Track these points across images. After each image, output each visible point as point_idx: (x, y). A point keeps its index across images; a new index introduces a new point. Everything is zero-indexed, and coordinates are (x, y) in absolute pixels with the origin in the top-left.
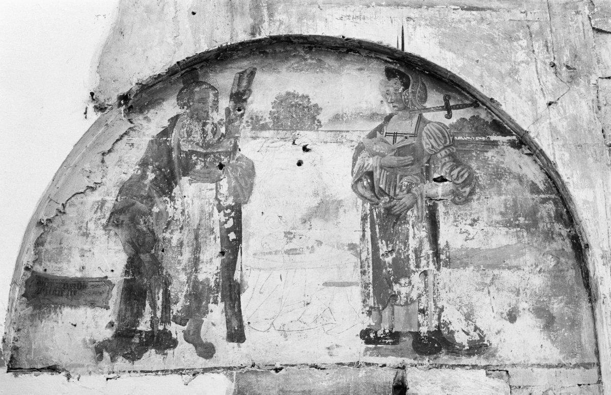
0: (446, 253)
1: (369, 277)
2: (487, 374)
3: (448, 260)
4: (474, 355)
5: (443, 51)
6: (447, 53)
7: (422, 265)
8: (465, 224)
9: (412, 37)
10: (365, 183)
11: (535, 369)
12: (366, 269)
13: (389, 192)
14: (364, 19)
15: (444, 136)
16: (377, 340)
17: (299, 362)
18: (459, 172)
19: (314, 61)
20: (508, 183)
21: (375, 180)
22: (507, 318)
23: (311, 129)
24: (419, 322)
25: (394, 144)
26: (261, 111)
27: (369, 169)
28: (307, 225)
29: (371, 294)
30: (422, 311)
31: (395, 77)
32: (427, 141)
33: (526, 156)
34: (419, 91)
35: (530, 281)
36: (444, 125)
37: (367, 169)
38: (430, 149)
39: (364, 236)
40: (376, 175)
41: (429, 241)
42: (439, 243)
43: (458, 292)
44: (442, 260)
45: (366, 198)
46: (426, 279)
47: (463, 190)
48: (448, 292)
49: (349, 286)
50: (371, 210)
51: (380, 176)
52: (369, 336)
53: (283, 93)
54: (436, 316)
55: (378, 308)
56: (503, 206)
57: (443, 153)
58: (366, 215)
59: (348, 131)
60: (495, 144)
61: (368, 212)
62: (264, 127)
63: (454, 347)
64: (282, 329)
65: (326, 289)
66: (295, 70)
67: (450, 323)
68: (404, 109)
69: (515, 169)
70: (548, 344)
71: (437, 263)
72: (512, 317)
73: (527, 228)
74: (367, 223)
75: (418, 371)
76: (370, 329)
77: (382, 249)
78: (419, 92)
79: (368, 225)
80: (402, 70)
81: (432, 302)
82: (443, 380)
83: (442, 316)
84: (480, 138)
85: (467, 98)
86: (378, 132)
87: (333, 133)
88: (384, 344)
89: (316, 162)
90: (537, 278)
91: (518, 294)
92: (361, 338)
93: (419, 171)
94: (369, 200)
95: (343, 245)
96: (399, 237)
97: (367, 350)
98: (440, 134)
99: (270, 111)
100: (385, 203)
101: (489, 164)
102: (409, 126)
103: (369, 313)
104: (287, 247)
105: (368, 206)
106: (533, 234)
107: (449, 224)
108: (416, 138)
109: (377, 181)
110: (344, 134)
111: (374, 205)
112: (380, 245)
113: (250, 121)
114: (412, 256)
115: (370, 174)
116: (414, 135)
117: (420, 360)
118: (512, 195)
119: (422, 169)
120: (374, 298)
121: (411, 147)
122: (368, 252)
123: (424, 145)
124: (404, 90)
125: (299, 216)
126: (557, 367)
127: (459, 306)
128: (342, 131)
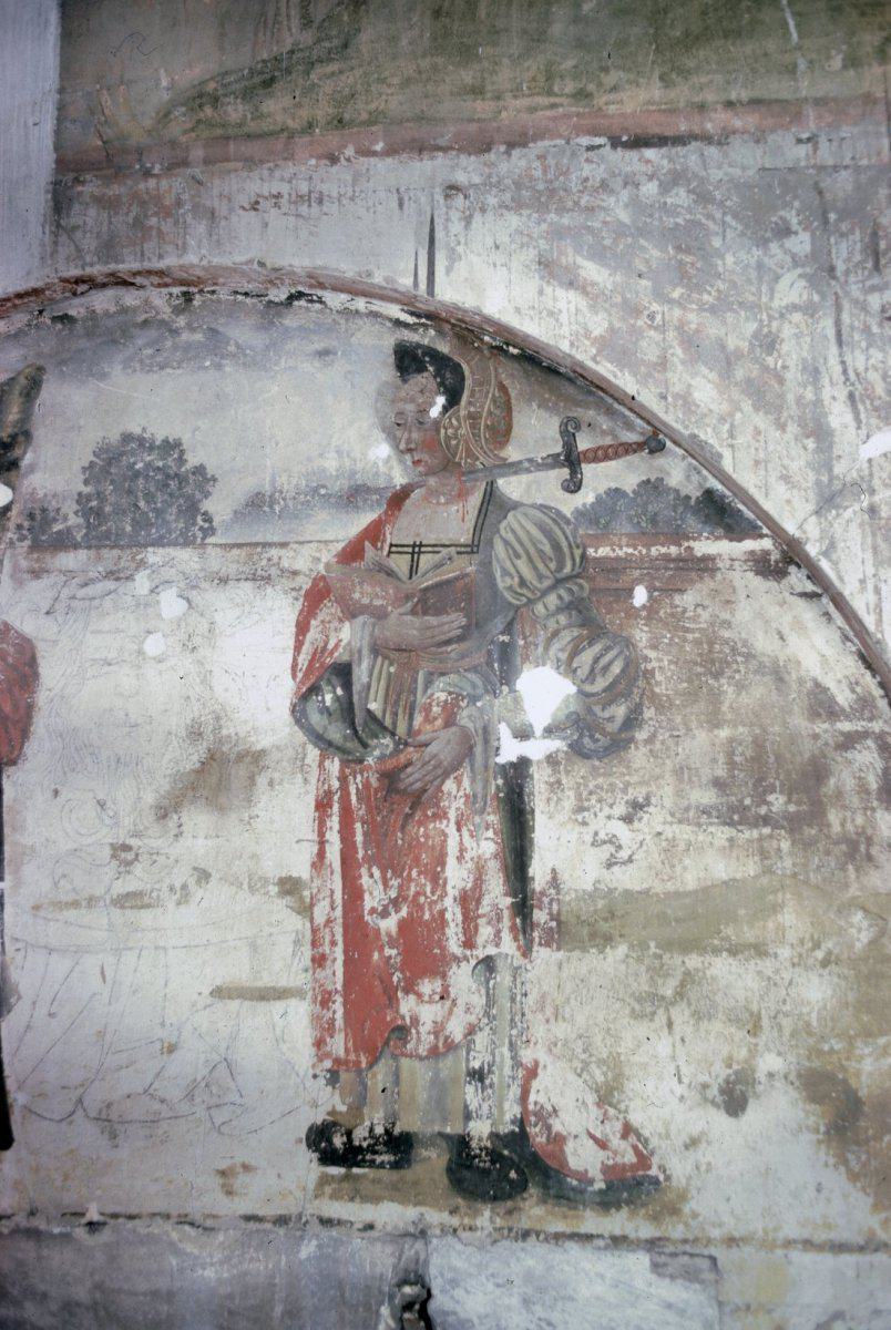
0: (550, 903)
1: (334, 974)
2: (655, 1267)
3: (554, 924)
4: (618, 1208)
5: (548, 290)
6: (561, 293)
7: (480, 940)
8: (609, 817)
9: (460, 249)
10: (328, 698)
11: (796, 1255)
12: (328, 951)
13: (395, 724)
14: (320, 202)
15: (556, 547)
16: (350, 1156)
17: (148, 1208)
18: (596, 660)
19: (198, 337)
20: (741, 687)
21: (356, 687)
22: (719, 1099)
23: (187, 542)
24: (466, 1107)
25: (411, 578)
26: (54, 496)
27: (340, 655)
28: (172, 823)
29: (339, 1022)
30: (478, 1076)
31: (421, 369)
32: (508, 564)
33: (801, 603)
34: (489, 410)
35: (793, 992)
36: (558, 513)
37: (336, 654)
38: (516, 593)
39: (321, 854)
40: (361, 674)
41: (505, 868)
42: (530, 875)
43: (580, 1019)
44: (538, 925)
45: (330, 744)
46: (492, 983)
47: (606, 714)
48: (552, 1020)
49: (279, 998)
50: (343, 779)
51: (371, 676)
52: (329, 1141)
53: (114, 436)
54: (515, 1091)
55: (358, 1063)
56: (722, 759)
57: (552, 600)
58: (329, 794)
59: (284, 545)
60: (706, 566)
61: (336, 784)
62: (63, 542)
63: (561, 1183)
64: (104, 1116)
65: (219, 1005)
66: (148, 368)
67: (555, 1111)
68: (445, 468)
69: (764, 644)
70: (836, 1180)
71: (524, 932)
72: (734, 1099)
73: (793, 824)
74: (331, 816)
75: (459, 1247)
76: (334, 1124)
77: (371, 894)
78: (490, 413)
79: (334, 822)
80: (444, 348)
81: (505, 1050)
82: (529, 1277)
83: (533, 1091)
84: (663, 550)
85: (629, 426)
86: (367, 543)
87: (243, 553)
88: (370, 1167)
89: (197, 640)
90: (815, 980)
91: (755, 1030)
92: (309, 1146)
93: (479, 658)
94: (338, 748)
95: (265, 881)
96: (417, 860)
97: (324, 1180)
98: (545, 541)
99: (80, 494)
100: (382, 758)
101: (687, 630)
102: (451, 521)
103: (333, 1078)
104: (121, 887)
105: (334, 766)
106: (808, 845)
107: (562, 817)
108: (476, 558)
109: (360, 693)
110: (274, 552)
111: (352, 761)
112: (365, 881)
113: (26, 524)
114: (454, 914)
115: (343, 672)
116: (472, 548)
117: (466, 1214)
118: (752, 725)
119: (489, 653)
120: (346, 1035)
121: (460, 584)
122: (332, 902)
123: (499, 580)
124: (445, 409)
125: (149, 798)
126: (861, 1249)
127: (582, 1061)
128: (271, 545)
